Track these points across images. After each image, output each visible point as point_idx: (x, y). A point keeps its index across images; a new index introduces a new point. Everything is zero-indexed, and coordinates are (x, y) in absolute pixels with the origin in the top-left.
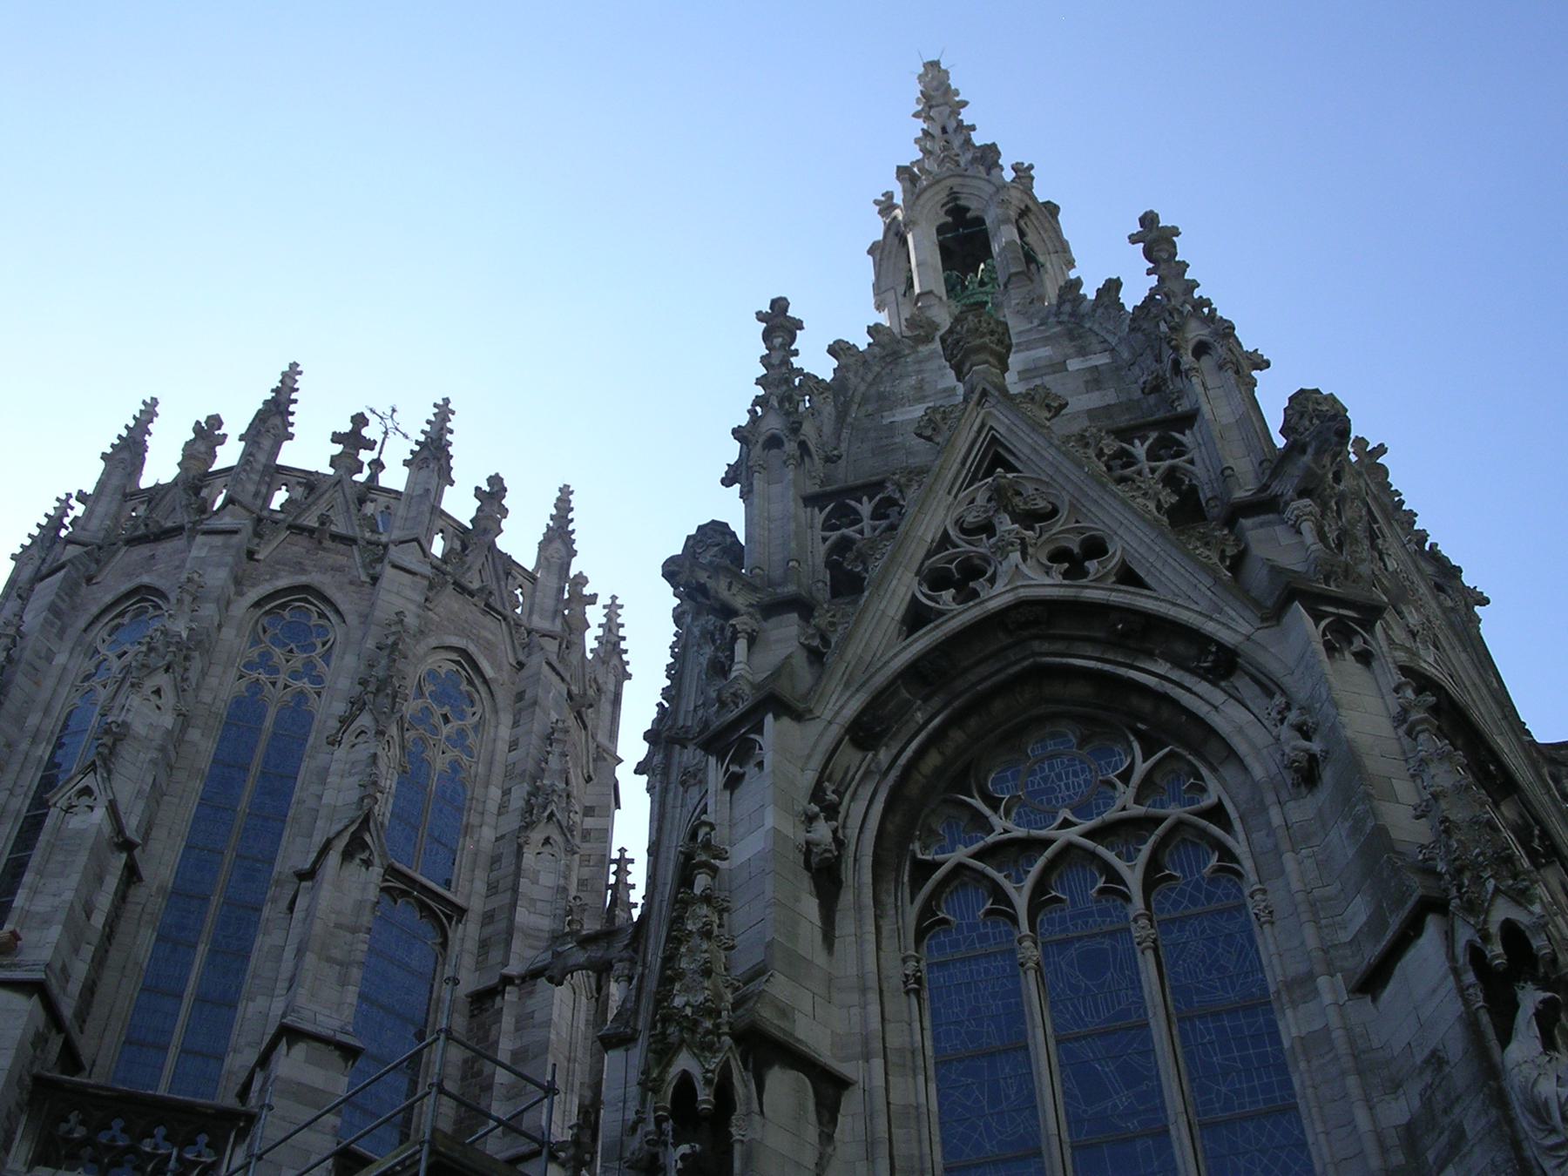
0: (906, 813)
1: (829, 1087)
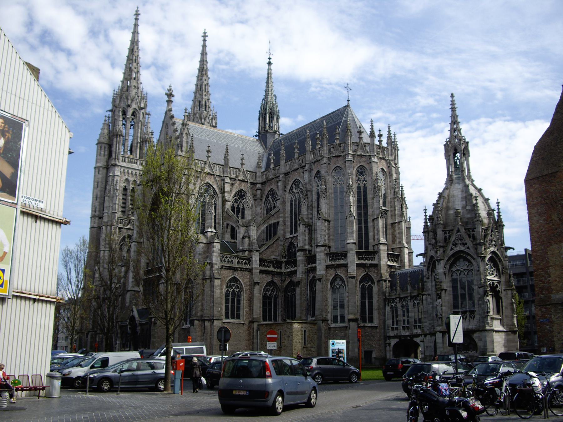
0: (451, 267)
1: (446, 290)
